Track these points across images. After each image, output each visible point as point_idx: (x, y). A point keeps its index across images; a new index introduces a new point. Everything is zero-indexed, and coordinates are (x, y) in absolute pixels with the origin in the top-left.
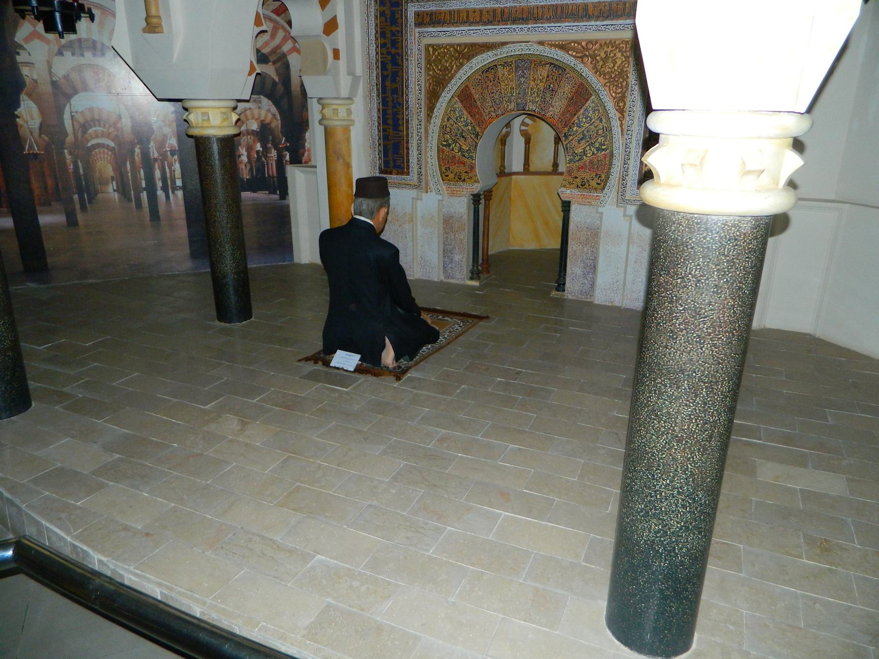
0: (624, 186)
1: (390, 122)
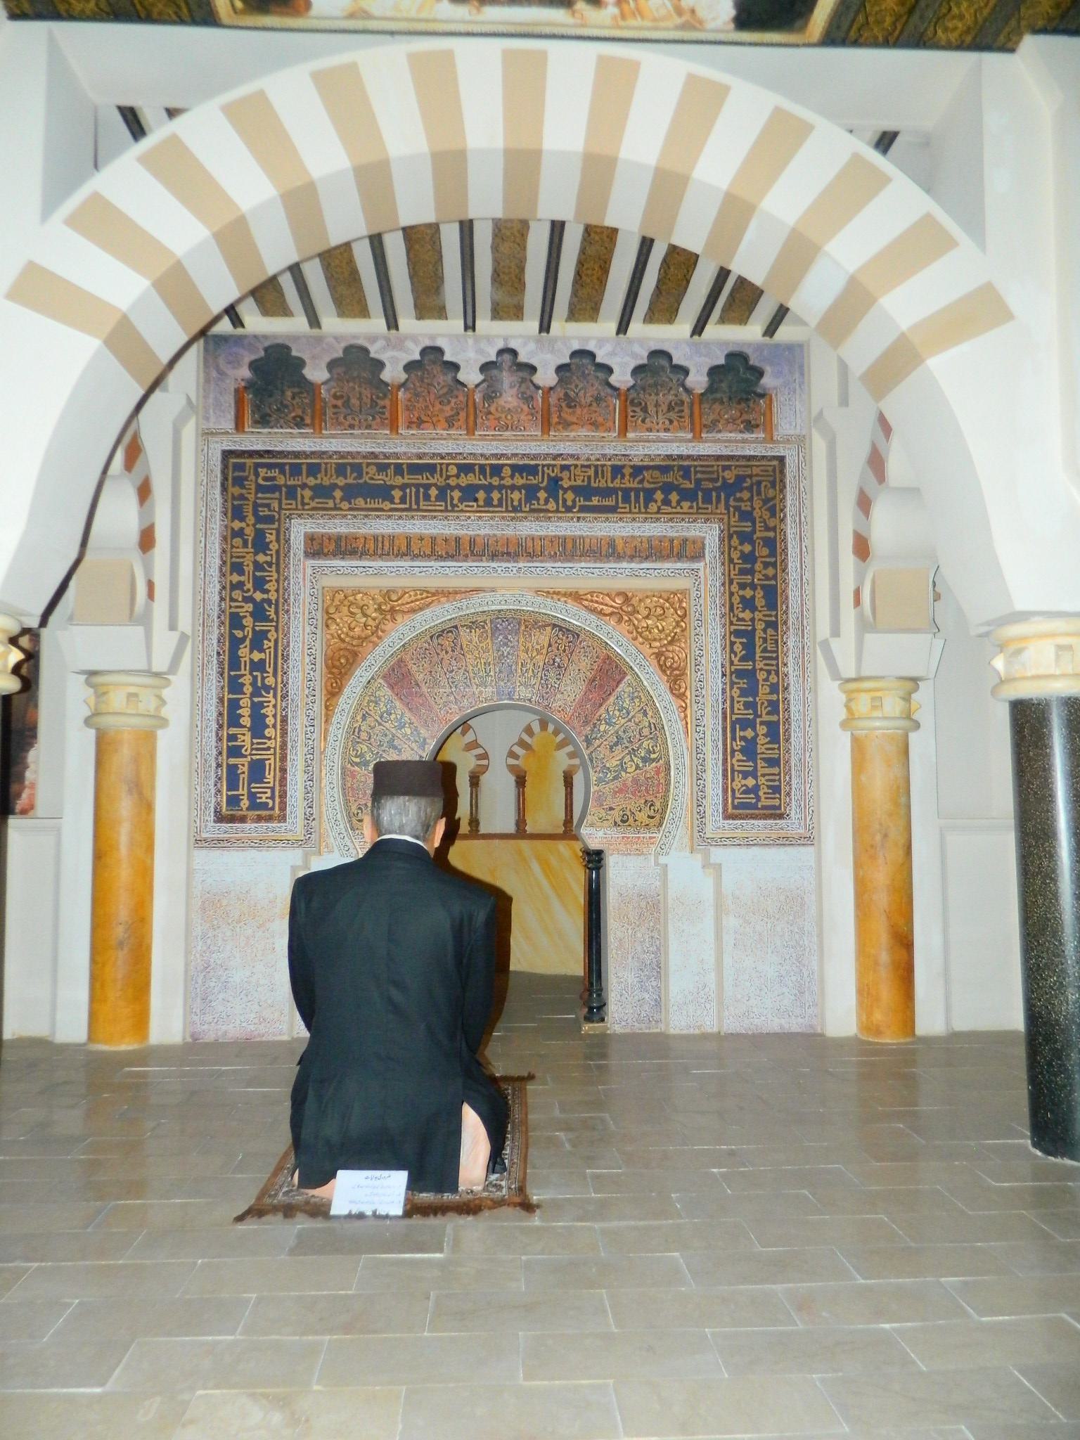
0: (702, 816)
1: (246, 721)
